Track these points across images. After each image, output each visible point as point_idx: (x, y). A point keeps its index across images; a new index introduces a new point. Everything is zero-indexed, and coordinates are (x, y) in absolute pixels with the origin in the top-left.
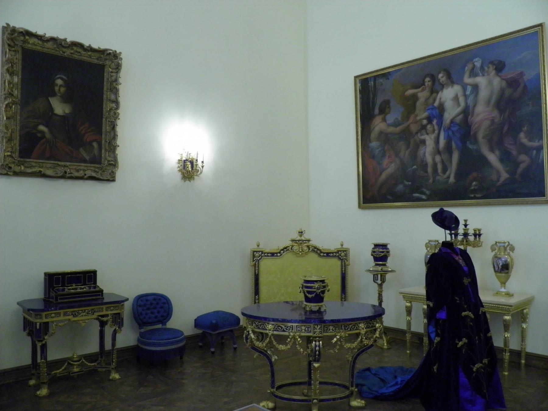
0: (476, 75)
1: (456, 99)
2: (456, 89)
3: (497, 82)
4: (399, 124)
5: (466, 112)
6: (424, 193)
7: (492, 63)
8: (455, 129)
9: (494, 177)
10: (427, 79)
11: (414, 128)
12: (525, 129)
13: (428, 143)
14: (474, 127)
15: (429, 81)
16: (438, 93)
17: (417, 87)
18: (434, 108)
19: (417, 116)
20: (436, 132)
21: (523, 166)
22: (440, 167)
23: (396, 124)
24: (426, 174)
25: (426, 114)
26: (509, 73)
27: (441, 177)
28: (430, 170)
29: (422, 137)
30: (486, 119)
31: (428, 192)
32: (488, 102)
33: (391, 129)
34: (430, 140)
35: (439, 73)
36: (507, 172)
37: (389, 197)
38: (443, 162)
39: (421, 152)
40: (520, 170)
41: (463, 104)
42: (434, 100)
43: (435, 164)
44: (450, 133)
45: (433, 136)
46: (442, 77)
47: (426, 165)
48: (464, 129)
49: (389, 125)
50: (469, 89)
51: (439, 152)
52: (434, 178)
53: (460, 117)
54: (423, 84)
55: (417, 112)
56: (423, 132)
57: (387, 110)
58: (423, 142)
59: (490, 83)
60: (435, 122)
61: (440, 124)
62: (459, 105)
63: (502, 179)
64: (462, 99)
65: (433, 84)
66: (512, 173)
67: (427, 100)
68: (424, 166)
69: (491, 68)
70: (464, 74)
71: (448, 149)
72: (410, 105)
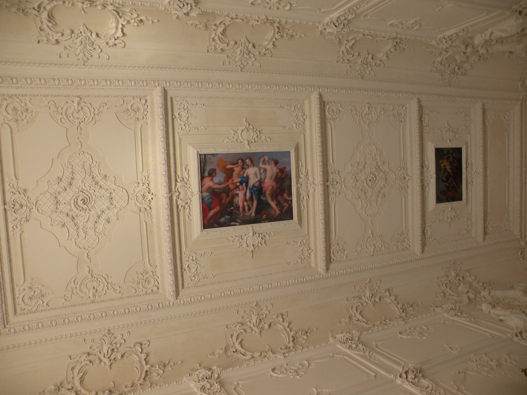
0: (266, 164)
1: (256, 174)
2: (256, 169)
3: (275, 169)
4: (222, 184)
5: (261, 182)
6: (238, 222)
7: (272, 159)
8: (255, 189)
9: (273, 213)
10: (240, 161)
11: (231, 187)
12: (286, 192)
13: (240, 195)
14: (264, 189)
16: (246, 169)
17: (234, 164)
18: (243, 177)
19: (233, 180)
20: (245, 190)
21: (285, 208)
23: (220, 184)
25: (239, 180)
26: (280, 165)
27: (247, 213)
28: (241, 209)
29: (237, 192)
31: (240, 221)
32: (271, 178)
33: (217, 186)
34: (241, 194)
36: (279, 210)
37: (215, 225)
38: (248, 205)
39: (236, 200)
40: (284, 210)
41: (259, 177)
42: (244, 173)
43: (244, 207)
44: (252, 191)
45: (243, 192)
46: (248, 161)
47: (239, 207)
48: (259, 191)
49: (215, 184)
50: (262, 170)
51: (246, 201)
52: (243, 214)
53: (258, 183)
54: (237, 163)
55: (233, 178)
56: (237, 189)
57: (214, 174)
58: (237, 195)
59: (272, 169)
60: (244, 184)
61: (247, 185)
62: (257, 177)
63: (277, 214)
64: (258, 175)
65: (243, 164)
66: (281, 211)
67: (240, 172)
68: (238, 208)
69: (273, 162)
70: (259, 162)
71: (251, 199)
72: (229, 174)
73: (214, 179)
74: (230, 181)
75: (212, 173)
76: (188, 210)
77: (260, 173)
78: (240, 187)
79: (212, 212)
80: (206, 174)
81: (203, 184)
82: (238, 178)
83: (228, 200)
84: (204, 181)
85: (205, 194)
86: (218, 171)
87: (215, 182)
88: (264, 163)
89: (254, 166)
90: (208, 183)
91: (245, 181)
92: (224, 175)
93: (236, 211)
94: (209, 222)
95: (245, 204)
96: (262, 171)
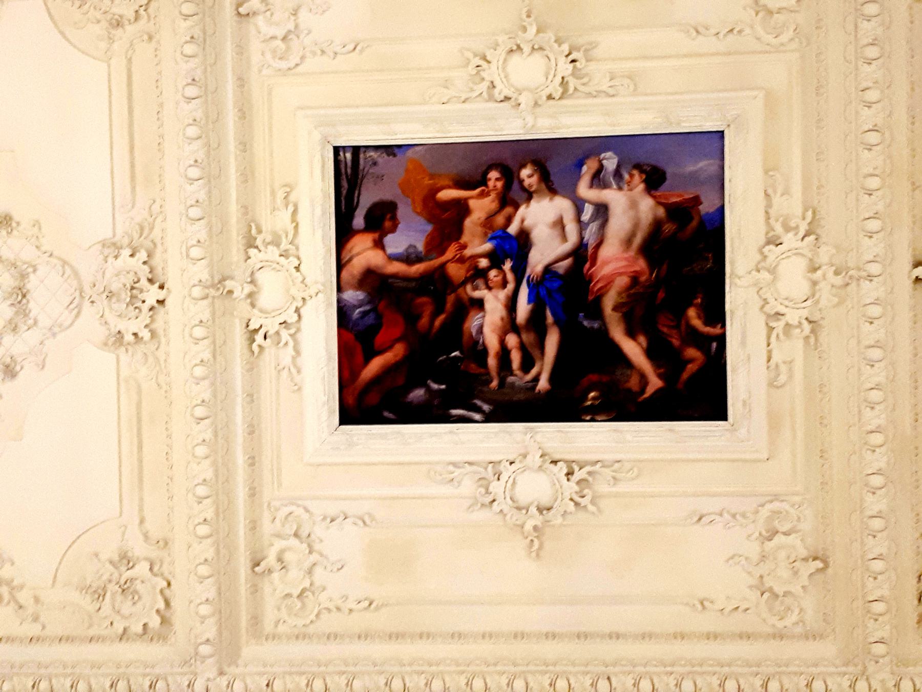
0: (605, 186)
1: (559, 224)
2: (561, 205)
4: (419, 259)
7: (638, 167)
10: (494, 175)
11: (456, 271)
13: (488, 306)
15: (497, 179)
16: (517, 207)
19: (464, 247)
20: (511, 286)
22: (516, 358)
23: (409, 258)
24: (482, 370)
25: (488, 246)
28: (492, 362)
29: (477, 294)
30: (621, 274)
32: (628, 242)
33: (397, 267)
35: (523, 166)
42: (509, 220)
43: (504, 354)
44: (543, 292)
45: (503, 295)
47: (485, 352)
49: (392, 258)
50: (588, 211)
54: (483, 181)
55: (465, 239)
56: (480, 282)
57: (388, 224)
58: (479, 304)
59: (633, 205)
60: (508, 265)
62: (564, 238)
65: (507, 187)
70: (579, 177)
71: (536, 323)
72: (447, 222)
73: (389, 239)
74: (450, 253)
75: (382, 219)
76: (290, 350)
77: (579, 220)
78: (493, 273)
79: (376, 365)
80: (359, 221)
81: (346, 256)
82: (486, 238)
83: (438, 323)
84: (349, 246)
85: (353, 296)
86: (404, 211)
87: (390, 250)
88: (598, 180)
89: (553, 191)
90: (365, 254)
91: (514, 248)
92: (429, 228)
93: (473, 368)
94: (362, 404)
95: (512, 340)
96: (586, 216)
